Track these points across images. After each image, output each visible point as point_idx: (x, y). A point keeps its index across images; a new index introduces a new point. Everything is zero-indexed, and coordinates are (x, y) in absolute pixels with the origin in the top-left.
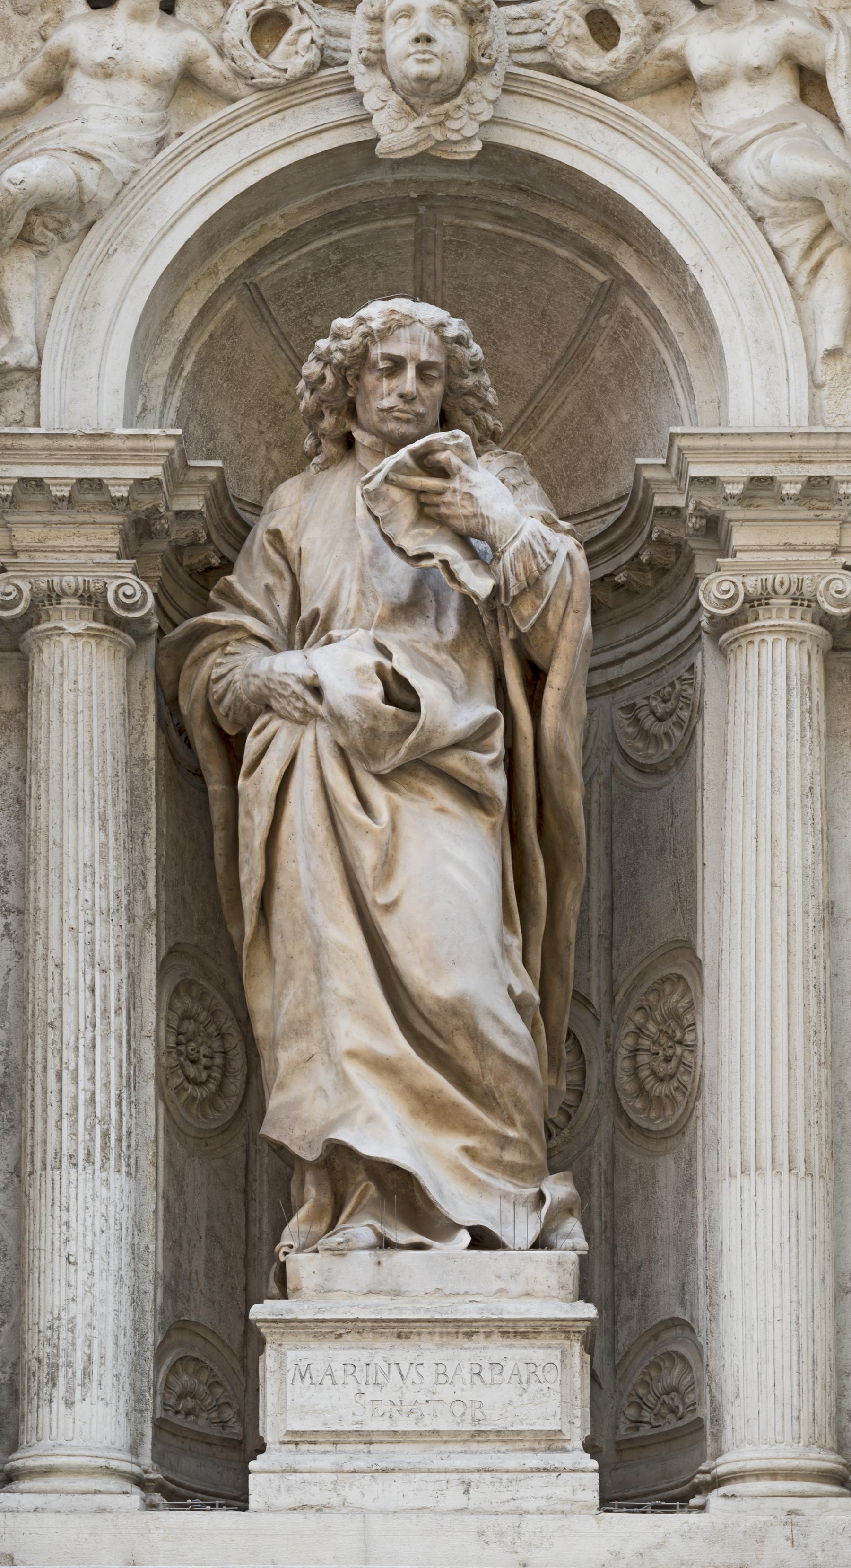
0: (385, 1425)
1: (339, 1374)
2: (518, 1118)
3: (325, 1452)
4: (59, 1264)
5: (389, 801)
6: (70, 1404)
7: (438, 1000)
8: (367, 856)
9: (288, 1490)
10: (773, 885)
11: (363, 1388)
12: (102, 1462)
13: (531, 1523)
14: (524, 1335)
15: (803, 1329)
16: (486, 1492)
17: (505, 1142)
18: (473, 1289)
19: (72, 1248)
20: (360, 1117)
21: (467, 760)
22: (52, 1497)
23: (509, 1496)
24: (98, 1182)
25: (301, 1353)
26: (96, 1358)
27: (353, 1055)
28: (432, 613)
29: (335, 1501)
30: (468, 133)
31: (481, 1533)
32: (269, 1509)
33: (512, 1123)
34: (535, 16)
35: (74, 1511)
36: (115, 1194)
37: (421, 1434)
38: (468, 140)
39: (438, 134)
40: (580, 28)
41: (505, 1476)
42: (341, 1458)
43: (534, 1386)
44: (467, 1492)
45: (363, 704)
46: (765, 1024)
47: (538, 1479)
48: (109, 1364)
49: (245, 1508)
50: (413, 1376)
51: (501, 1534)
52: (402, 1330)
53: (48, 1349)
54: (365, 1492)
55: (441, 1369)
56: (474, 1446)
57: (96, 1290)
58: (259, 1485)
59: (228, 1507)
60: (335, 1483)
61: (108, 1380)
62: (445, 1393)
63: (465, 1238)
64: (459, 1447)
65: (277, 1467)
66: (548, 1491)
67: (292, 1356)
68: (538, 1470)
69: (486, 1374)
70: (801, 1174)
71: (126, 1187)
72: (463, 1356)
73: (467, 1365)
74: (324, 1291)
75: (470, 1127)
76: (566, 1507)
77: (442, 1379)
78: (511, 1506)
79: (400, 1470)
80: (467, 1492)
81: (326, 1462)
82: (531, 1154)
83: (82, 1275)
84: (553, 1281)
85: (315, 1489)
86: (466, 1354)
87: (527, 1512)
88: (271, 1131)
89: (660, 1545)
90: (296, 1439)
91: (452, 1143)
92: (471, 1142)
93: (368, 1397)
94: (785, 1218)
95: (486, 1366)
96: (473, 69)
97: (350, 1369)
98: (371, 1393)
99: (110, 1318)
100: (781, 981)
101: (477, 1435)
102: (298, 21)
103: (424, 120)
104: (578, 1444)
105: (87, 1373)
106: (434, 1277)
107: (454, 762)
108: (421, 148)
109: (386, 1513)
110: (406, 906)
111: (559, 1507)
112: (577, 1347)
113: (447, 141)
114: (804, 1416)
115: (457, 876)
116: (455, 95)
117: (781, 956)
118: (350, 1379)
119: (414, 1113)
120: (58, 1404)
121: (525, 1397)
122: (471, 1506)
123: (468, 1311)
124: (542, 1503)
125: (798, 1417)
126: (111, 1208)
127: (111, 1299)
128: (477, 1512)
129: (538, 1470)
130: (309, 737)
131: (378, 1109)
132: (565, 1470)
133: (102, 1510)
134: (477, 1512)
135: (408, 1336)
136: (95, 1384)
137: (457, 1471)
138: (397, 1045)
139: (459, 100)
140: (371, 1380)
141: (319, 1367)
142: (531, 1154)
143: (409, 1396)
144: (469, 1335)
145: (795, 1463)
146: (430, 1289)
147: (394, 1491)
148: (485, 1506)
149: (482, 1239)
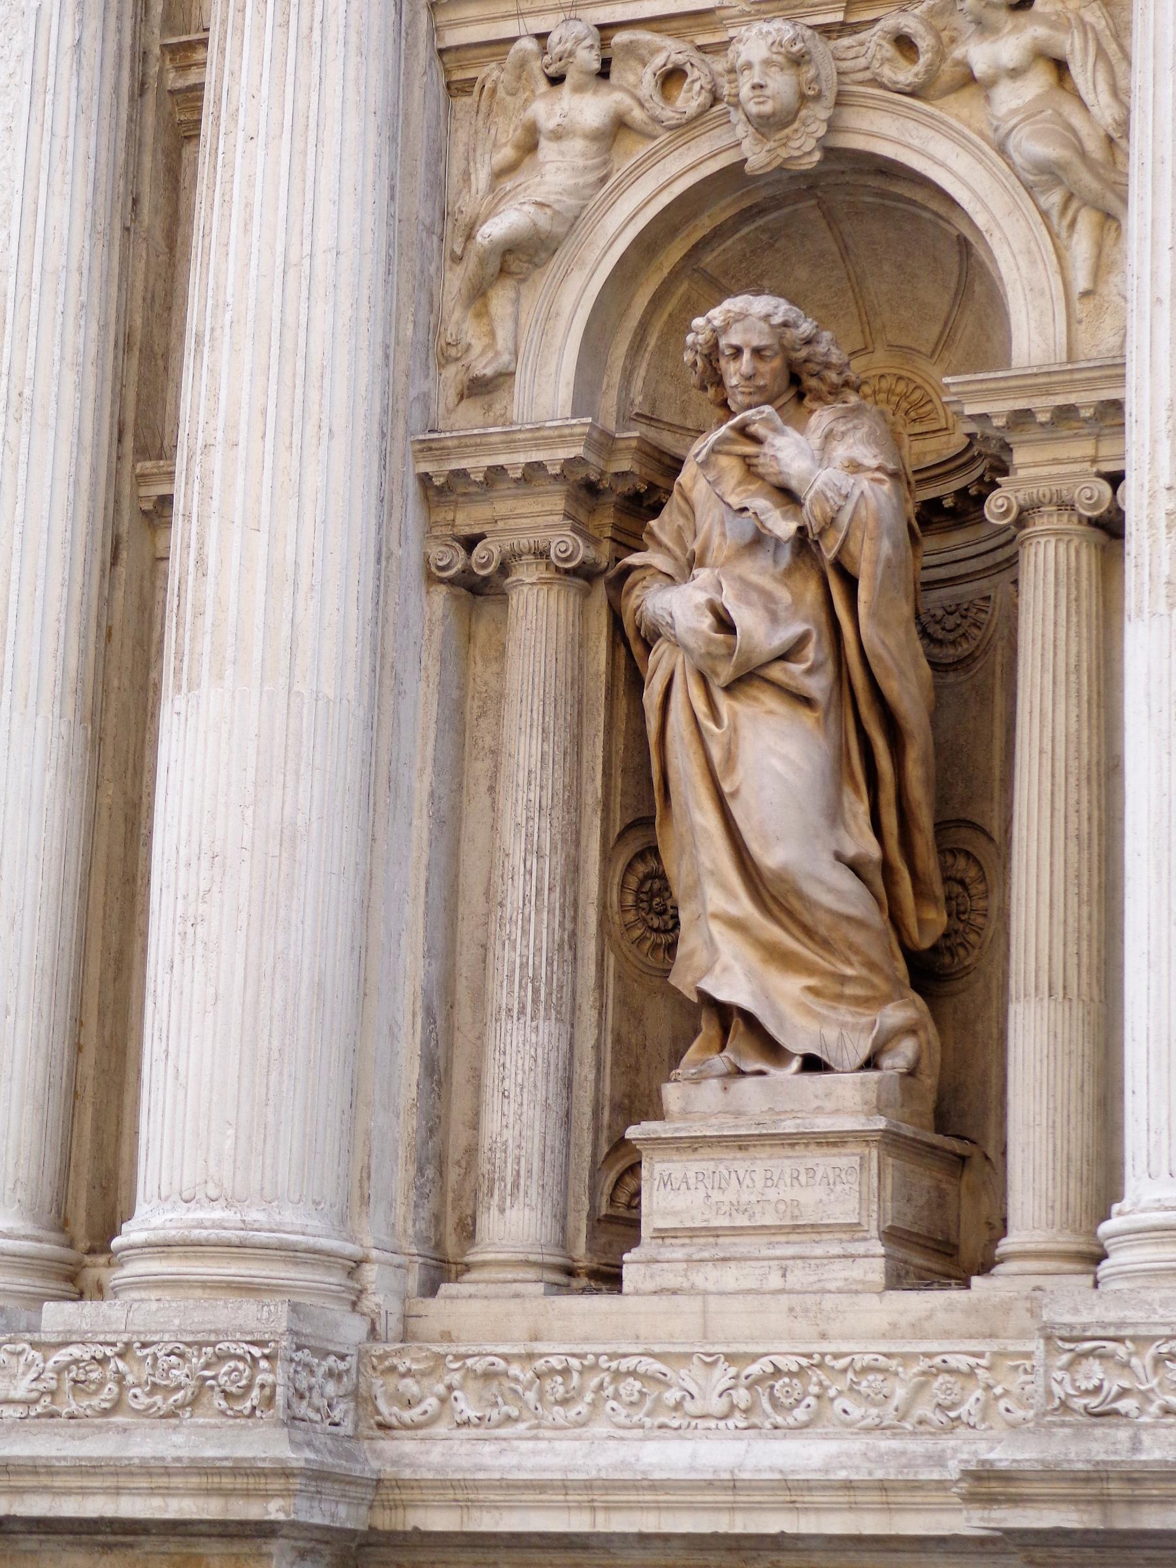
0: (724, 1222)
1: (692, 1181)
2: (854, 958)
3: (683, 1245)
4: (497, 1097)
5: (731, 708)
6: (502, 1211)
7: (770, 869)
8: (717, 754)
9: (652, 1277)
10: (1041, 752)
11: (710, 1192)
12: (521, 1257)
13: (829, 1302)
14: (834, 1144)
15: (1059, 1132)
16: (799, 1277)
17: (843, 979)
18: (796, 1107)
19: (506, 1083)
20: (718, 968)
21: (785, 670)
22: (482, 1286)
23: (816, 1278)
24: (528, 1030)
25: (665, 1166)
26: (522, 1173)
27: (715, 916)
28: (772, 549)
29: (686, 1285)
30: (807, 148)
31: (791, 1310)
32: (637, 1293)
33: (850, 963)
34: (862, 44)
35: (497, 1297)
36: (543, 1037)
37: (754, 1228)
38: (810, 153)
39: (784, 153)
40: (889, 50)
41: (813, 1262)
42: (692, 1250)
43: (839, 1187)
44: (784, 1276)
45: (695, 631)
46: (1033, 870)
47: (838, 1265)
48: (535, 1177)
49: (620, 1292)
50: (748, 1181)
51: (807, 1310)
52: (741, 1143)
53: (489, 1167)
54: (708, 1277)
55: (769, 1175)
56: (793, 1237)
57: (524, 1118)
58: (630, 1274)
59: (610, 1291)
60: (686, 1270)
61: (534, 1191)
62: (771, 1194)
63: (796, 1064)
64: (783, 1238)
65: (643, 1258)
66: (846, 1274)
67: (658, 1167)
68: (839, 1257)
69: (803, 1178)
70: (1060, 999)
71: (556, 1032)
72: (784, 1164)
73: (788, 1171)
74: (685, 1114)
75: (809, 969)
76: (860, 1287)
77: (769, 1183)
78: (816, 1287)
79: (735, 1259)
80: (784, 1276)
81: (680, 1254)
82: (873, 986)
83: (514, 1106)
84: (858, 1099)
85: (671, 1276)
86: (787, 1162)
87: (830, 1292)
88: (673, 980)
89: (929, 1317)
90: (662, 1234)
91: (792, 985)
92: (812, 982)
93: (714, 1199)
94: (1045, 1037)
95: (802, 1171)
96: (803, 98)
97: (701, 1177)
98: (716, 1196)
99: (536, 1140)
100: (1046, 834)
101: (795, 1228)
102: (693, 74)
103: (772, 144)
104: (874, 1233)
105: (516, 1185)
106: (775, 1096)
107: (776, 672)
108: (775, 164)
109: (721, 1293)
110: (745, 793)
111: (854, 1287)
112: (874, 1153)
113: (791, 158)
114: (1058, 1206)
115: (779, 766)
116: (793, 121)
117: (1047, 813)
118: (700, 1185)
119: (765, 961)
120: (494, 1211)
121: (832, 1197)
122: (788, 1287)
123: (789, 1126)
124: (840, 1284)
125: (1053, 1207)
126: (540, 1050)
127: (537, 1124)
128: (791, 1292)
129: (839, 1257)
130: (680, 659)
131: (732, 962)
132: (859, 1256)
133: (517, 1296)
134: (791, 1292)
135: (746, 1148)
136: (522, 1194)
137: (778, 1258)
138: (745, 907)
139: (796, 125)
140: (716, 1185)
141: (677, 1175)
142: (873, 986)
143: (745, 1198)
144: (792, 1145)
145: (1042, 1247)
146: (765, 1108)
147: (730, 1277)
148: (798, 1287)
149: (812, 1064)
